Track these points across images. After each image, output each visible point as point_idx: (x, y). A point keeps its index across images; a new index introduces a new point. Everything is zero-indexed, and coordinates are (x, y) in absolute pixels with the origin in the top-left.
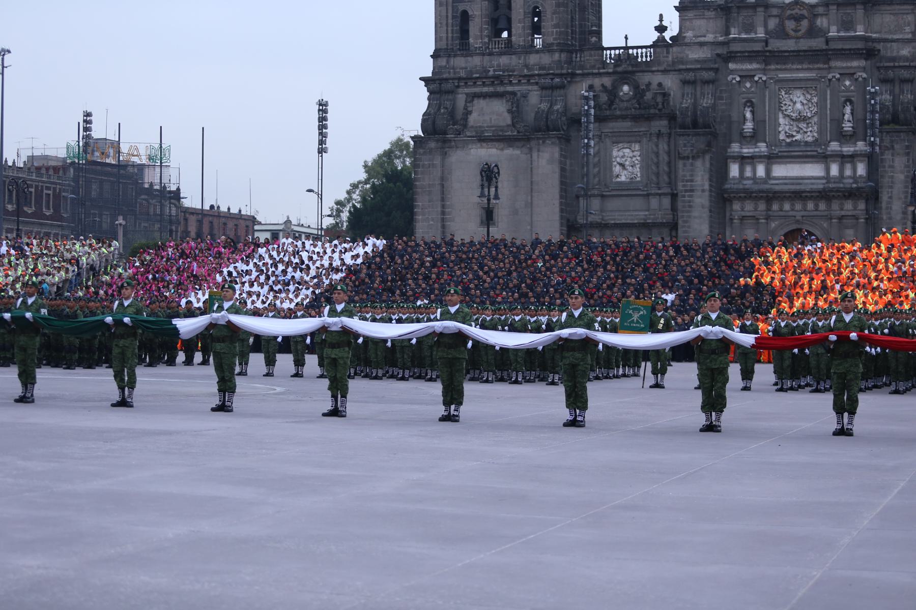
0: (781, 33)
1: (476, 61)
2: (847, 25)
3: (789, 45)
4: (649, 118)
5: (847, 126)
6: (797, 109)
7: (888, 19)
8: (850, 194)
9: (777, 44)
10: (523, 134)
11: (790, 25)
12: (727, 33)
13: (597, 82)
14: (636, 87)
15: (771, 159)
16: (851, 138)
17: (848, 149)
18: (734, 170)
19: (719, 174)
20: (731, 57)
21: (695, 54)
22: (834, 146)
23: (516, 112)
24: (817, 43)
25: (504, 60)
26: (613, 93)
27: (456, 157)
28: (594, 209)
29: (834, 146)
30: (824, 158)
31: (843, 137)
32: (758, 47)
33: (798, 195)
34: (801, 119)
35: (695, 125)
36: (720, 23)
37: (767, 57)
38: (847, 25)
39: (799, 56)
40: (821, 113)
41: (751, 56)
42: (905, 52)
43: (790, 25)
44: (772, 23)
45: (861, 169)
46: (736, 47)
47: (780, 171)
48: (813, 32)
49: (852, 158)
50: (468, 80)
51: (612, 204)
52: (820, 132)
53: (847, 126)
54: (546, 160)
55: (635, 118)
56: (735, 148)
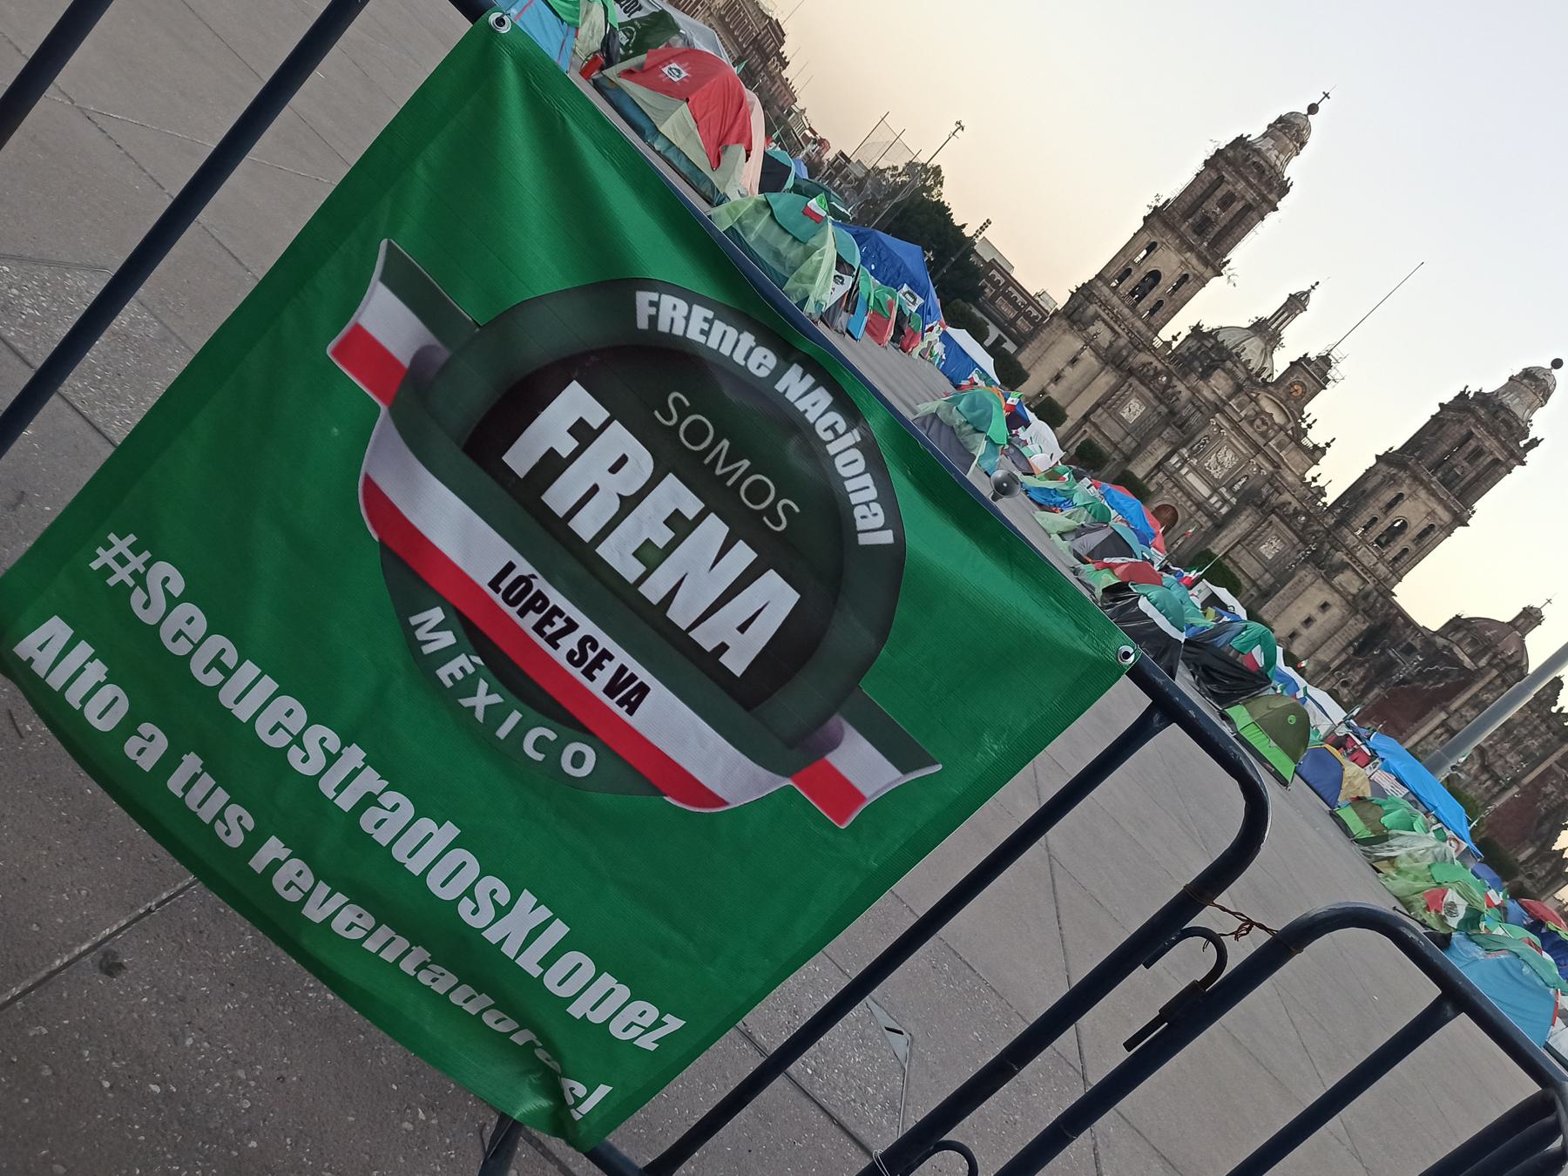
0: (1251, 423)
1: (1115, 300)
2: (1281, 446)
3: (1249, 430)
4: (1161, 402)
5: (1237, 487)
6: (1223, 459)
7: (1298, 458)
8: (1210, 515)
9: (1244, 424)
10: (1112, 359)
11: (1258, 422)
12: (1230, 398)
13: (1156, 363)
14: (1169, 380)
15: (1194, 469)
16: (1234, 494)
17: (1228, 496)
18: (1174, 460)
19: (1168, 457)
20: (1222, 412)
21: (1207, 393)
22: (1223, 490)
23: (1111, 344)
24: (1261, 441)
25: (1126, 311)
26: (1157, 374)
27: (1068, 338)
28: (1100, 416)
29: (1223, 490)
30: (1215, 491)
31: (1230, 489)
32: (1236, 419)
33: (1189, 496)
34: (1221, 465)
35: (1180, 427)
36: (1230, 391)
37: (1236, 426)
38: (1281, 446)
39: (1248, 438)
40: (1231, 471)
41: (1230, 420)
42: (1290, 479)
43: (1258, 422)
44: (1251, 413)
45: (1224, 510)
46: (1227, 409)
47: (1192, 478)
48: (1263, 435)
49: (1225, 501)
50: (1104, 304)
51: (1110, 422)
52: (1224, 478)
53: (1237, 487)
54: (1106, 380)
55: (1156, 397)
56: (1184, 451)
